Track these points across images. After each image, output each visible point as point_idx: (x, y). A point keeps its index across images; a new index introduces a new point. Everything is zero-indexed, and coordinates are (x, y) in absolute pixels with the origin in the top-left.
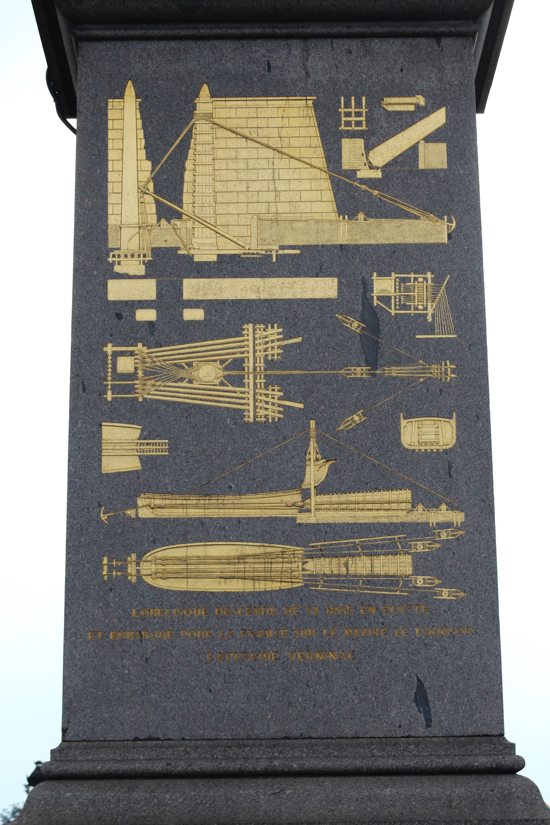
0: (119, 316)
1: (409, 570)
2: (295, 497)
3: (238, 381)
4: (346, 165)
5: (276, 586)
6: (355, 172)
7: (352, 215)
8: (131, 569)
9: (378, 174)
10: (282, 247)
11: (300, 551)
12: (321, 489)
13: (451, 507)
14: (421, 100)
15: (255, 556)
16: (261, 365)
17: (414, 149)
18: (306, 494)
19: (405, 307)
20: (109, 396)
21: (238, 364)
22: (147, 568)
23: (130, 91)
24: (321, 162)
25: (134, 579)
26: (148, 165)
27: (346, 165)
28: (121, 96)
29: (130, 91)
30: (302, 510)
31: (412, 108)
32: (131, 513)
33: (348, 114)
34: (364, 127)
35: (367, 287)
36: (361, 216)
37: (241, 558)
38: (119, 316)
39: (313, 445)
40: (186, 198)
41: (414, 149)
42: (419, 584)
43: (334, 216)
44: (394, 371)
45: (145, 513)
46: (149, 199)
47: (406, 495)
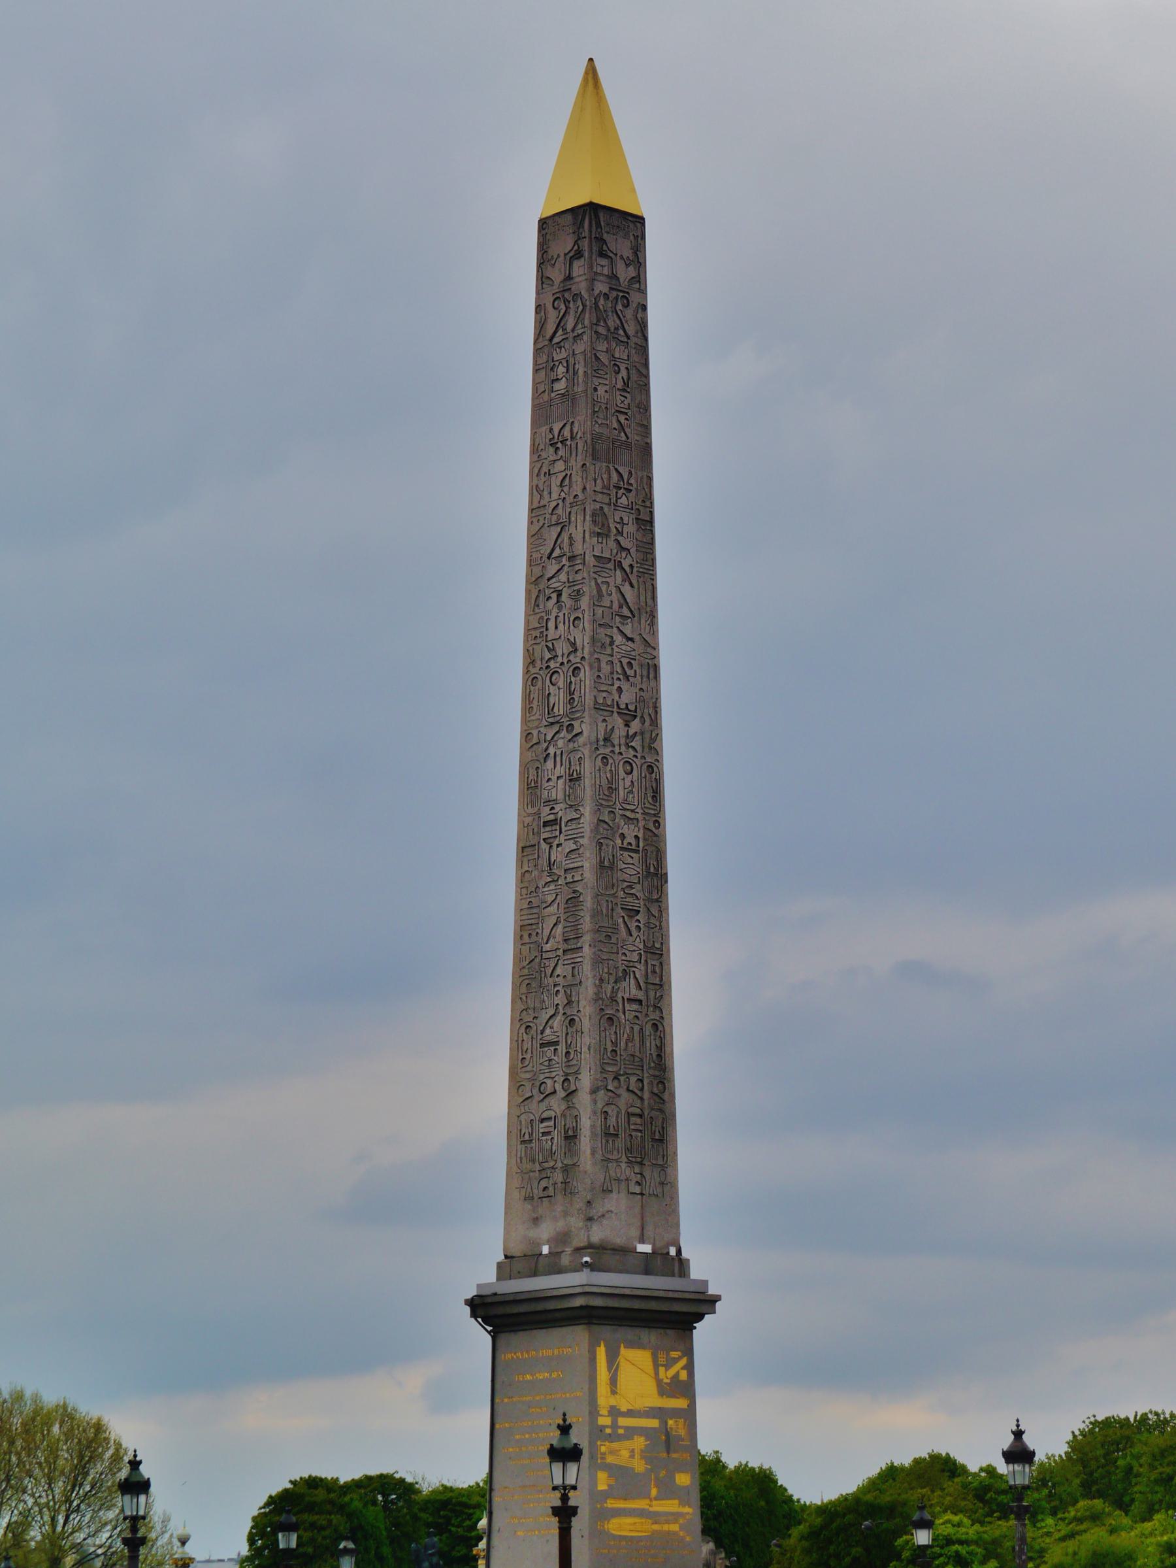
0: (601, 1431)
1: (678, 1529)
2: (647, 1501)
3: (632, 1456)
4: (661, 1377)
5: (644, 1534)
6: (663, 1379)
7: (662, 1396)
8: (606, 1526)
9: (668, 1381)
10: (644, 1407)
11: (650, 1521)
12: (656, 1499)
13: (689, 1507)
14: (679, 1353)
15: (638, 1523)
16: (639, 1451)
17: (677, 1374)
18: (651, 1500)
19: (676, 1432)
20: (599, 1461)
21: (633, 1451)
22: (611, 1526)
23: (602, 1344)
24: (653, 1375)
25: (606, 1530)
26: (608, 1373)
27: (661, 1377)
28: (600, 1346)
29: (602, 1344)
30: (650, 1506)
31: (677, 1356)
32: (605, 1505)
33: (661, 1358)
34: (665, 1363)
35: (666, 1423)
36: (664, 1396)
37: (635, 1523)
38: (601, 1431)
39: (653, 1484)
40: (618, 1386)
41: (678, 1372)
42: (681, 1535)
43: (656, 1396)
44: (674, 1455)
45: (609, 1506)
46: (608, 1387)
47: (676, 1502)
